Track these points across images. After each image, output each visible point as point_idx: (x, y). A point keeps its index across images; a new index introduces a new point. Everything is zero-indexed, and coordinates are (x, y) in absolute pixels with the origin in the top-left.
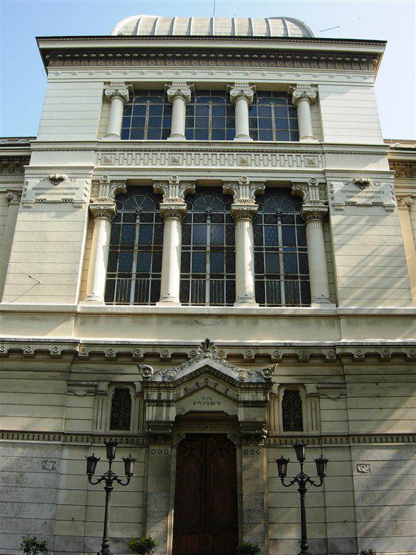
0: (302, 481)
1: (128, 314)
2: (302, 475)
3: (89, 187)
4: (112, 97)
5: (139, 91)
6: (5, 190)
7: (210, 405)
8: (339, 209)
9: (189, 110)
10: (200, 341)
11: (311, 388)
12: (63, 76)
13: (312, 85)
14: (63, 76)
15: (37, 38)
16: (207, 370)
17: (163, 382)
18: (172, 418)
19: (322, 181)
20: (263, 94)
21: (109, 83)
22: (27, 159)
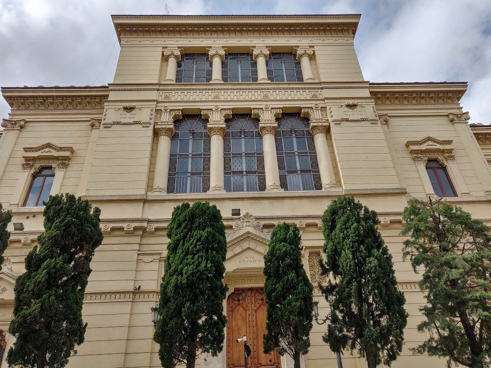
3: (154, 113)
5: (187, 55)
6: (89, 119)
8: (339, 122)
9: (224, 64)
13: (310, 47)
15: (112, 16)
20: (275, 54)
21: (167, 47)
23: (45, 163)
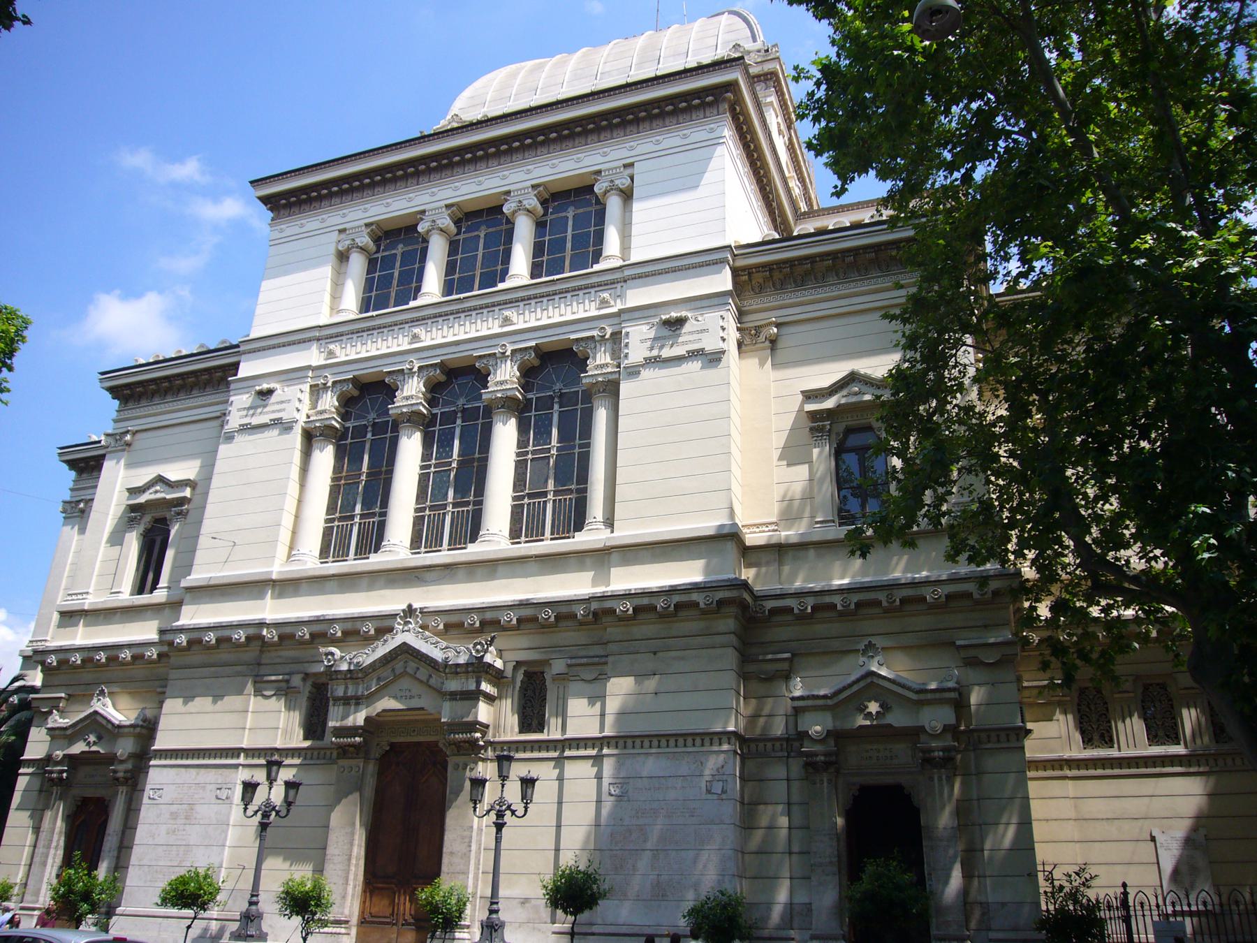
0: (501, 814)
1: (333, 575)
2: (501, 801)
3: (306, 397)
4: (349, 249)
6: (218, 414)
8: (634, 372)
10: (400, 606)
11: (558, 666)
12: (288, 232)
13: (625, 166)
14: (288, 232)
15: (251, 182)
16: (405, 649)
17: (349, 671)
19: (616, 329)
22: (235, 367)
23: (159, 515)
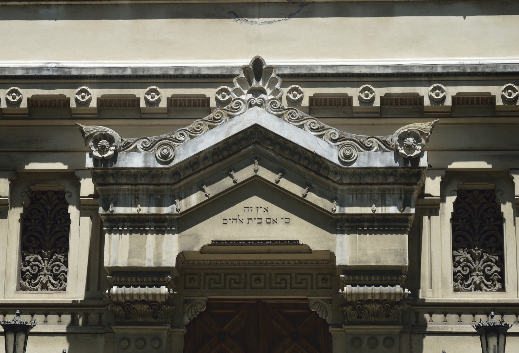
7: (265, 226)
18: (169, 260)
